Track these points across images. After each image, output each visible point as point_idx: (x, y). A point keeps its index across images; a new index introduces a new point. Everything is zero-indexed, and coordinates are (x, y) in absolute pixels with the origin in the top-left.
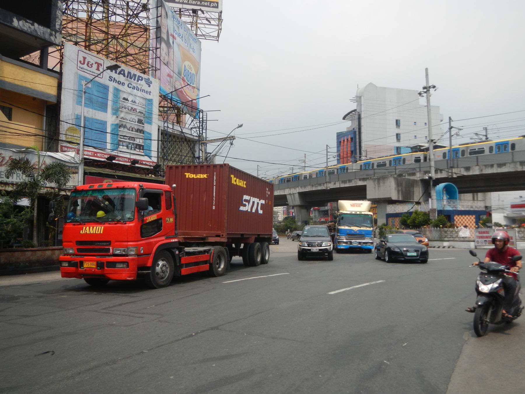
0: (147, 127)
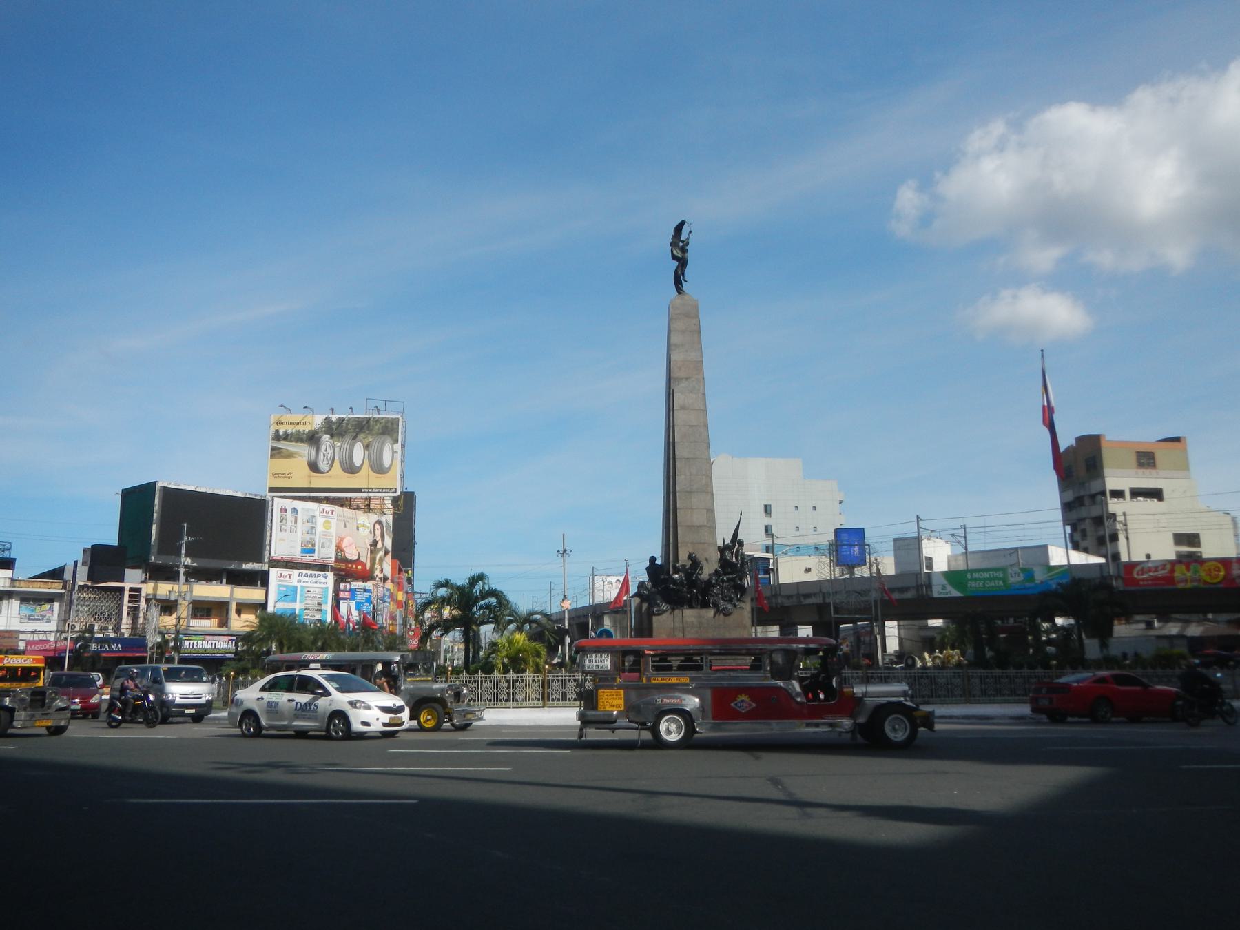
0: (323, 607)
